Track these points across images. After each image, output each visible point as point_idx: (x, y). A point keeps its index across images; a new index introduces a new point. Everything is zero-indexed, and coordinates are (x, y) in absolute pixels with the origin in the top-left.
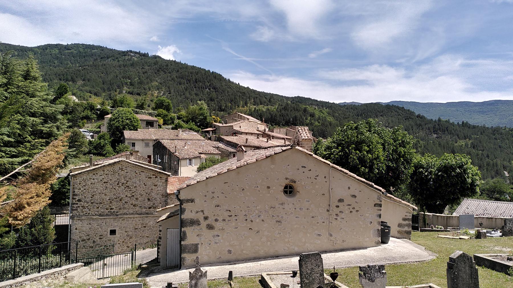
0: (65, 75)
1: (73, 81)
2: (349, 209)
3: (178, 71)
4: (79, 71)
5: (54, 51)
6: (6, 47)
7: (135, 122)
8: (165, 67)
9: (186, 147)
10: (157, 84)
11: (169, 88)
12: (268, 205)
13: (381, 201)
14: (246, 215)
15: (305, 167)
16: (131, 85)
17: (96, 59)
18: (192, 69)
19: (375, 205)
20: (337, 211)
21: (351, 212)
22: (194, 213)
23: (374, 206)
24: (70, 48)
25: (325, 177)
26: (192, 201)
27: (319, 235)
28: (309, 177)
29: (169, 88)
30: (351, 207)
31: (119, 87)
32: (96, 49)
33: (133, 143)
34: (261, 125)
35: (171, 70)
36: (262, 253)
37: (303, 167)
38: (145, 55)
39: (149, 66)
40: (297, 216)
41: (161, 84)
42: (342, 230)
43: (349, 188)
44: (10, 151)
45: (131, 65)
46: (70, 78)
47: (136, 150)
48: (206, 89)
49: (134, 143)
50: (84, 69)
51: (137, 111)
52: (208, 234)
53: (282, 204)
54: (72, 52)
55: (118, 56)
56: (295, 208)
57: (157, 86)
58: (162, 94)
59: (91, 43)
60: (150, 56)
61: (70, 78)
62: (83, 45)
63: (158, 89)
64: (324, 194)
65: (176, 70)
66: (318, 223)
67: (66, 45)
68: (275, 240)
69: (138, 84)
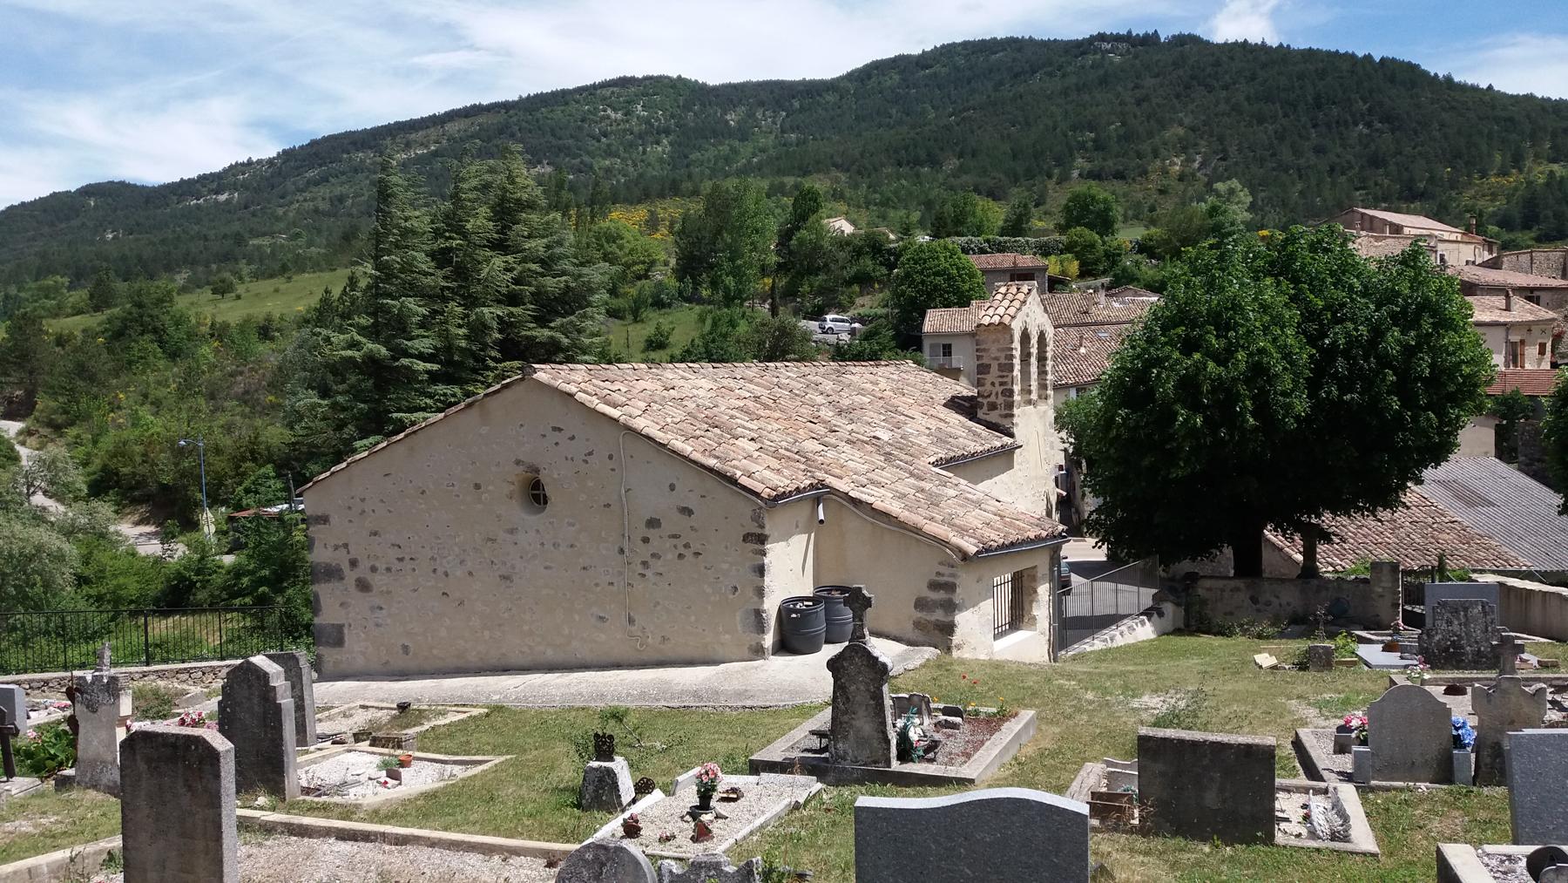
0: (911, 148)
1: (934, 162)
2: (675, 547)
3: (1253, 78)
4: (948, 128)
5: (887, 78)
6: (772, 92)
7: (963, 281)
8: (1209, 70)
9: (1083, 350)
10: (1181, 131)
11: (1221, 139)
12: (480, 534)
13: (762, 527)
14: (433, 558)
15: (560, 430)
16: (1096, 150)
17: (1001, 83)
18: (1305, 63)
19: (747, 538)
20: (644, 552)
21: (681, 556)
22: (330, 549)
23: (744, 540)
24: (930, 62)
25: (611, 457)
26: (324, 520)
27: (601, 618)
28: (569, 457)
29: (1221, 139)
30: (680, 543)
31: (1060, 162)
32: (1002, 51)
33: (944, 346)
34: (1455, 245)
35: (1231, 78)
36: (472, 659)
37: (555, 429)
38: (1150, 40)
39: (1157, 76)
40: (548, 564)
41: (1193, 129)
42: (659, 608)
43: (672, 487)
44: (445, 395)
45: (1101, 84)
46: (923, 155)
47: (955, 365)
48: (1357, 125)
49: (950, 345)
50: (963, 119)
51: (1000, 242)
52: (359, 601)
53: (512, 531)
54: (935, 73)
55: (1063, 59)
56: (542, 544)
57: (1180, 140)
58: (1196, 165)
59: (1001, 34)
60: (1162, 40)
61: (923, 155)
62: (965, 44)
63: (1184, 149)
64: (608, 505)
65: (1248, 74)
66: (597, 585)
67: (920, 56)
68: (500, 625)
69: (1119, 141)
